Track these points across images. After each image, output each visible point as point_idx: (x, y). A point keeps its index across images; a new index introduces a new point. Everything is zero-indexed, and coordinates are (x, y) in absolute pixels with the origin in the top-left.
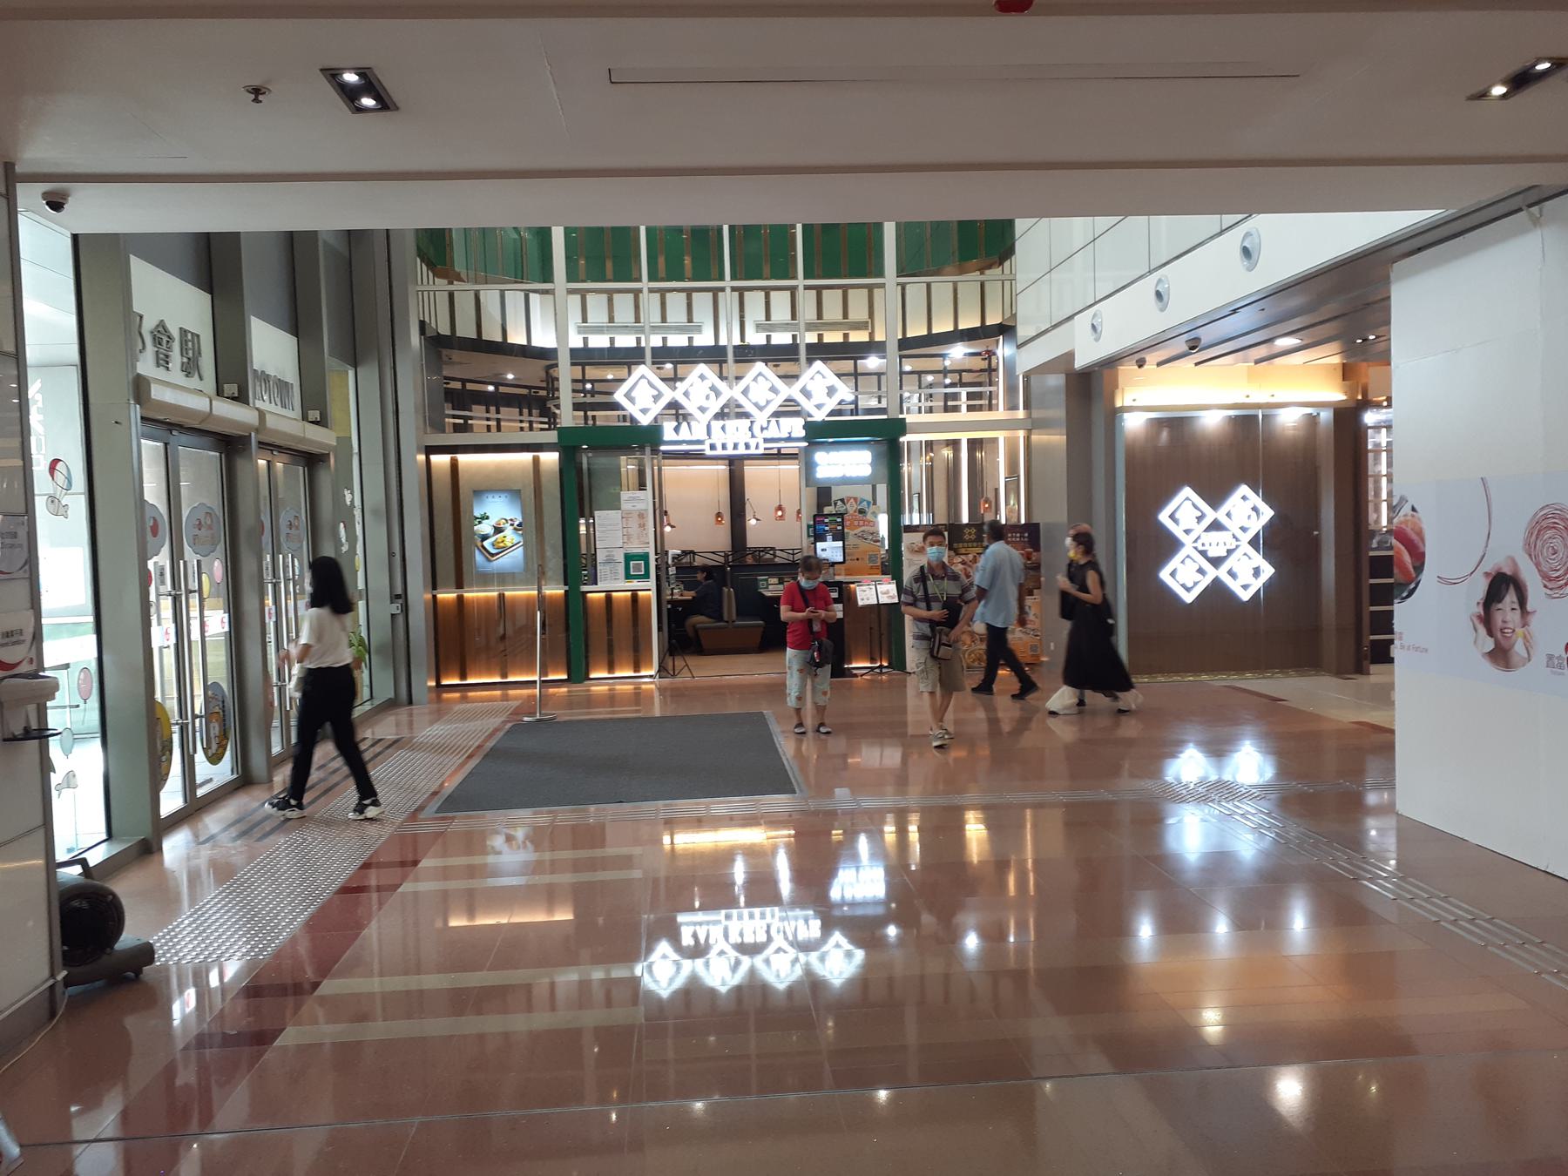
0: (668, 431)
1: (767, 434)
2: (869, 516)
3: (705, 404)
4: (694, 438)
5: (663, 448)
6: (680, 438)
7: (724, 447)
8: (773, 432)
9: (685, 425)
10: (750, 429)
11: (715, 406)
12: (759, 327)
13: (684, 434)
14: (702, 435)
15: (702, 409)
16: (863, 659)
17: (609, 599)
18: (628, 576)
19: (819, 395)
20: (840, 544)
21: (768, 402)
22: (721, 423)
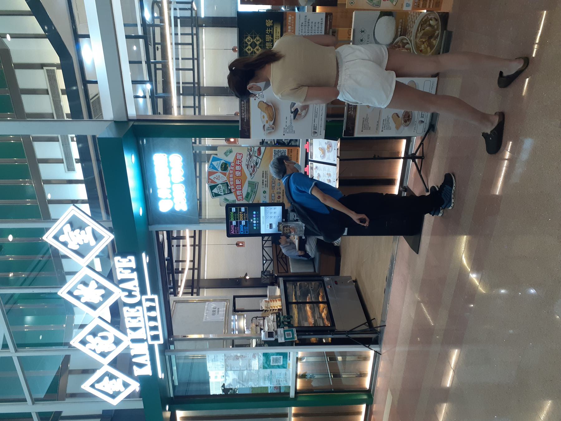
0: (147, 371)
1: (137, 292)
2: (230, 159)
3: (111, 339)
4: (147, 352)
5: (161, 375)
6: (149, 363)
7: (155, 328)
8: (134, 285)
9: (134, 360)
10: (132, 306)
11: (112, 332)
12: (70, 168)
13: (145, 359)
14: (143, 348)
15: (117, 342)
16: (392, 168)
17: (303, 376)
18: (284, 367)
19: (85, 237)
20: (262, 209)
21: (100, 287)
22: (129, 331)
